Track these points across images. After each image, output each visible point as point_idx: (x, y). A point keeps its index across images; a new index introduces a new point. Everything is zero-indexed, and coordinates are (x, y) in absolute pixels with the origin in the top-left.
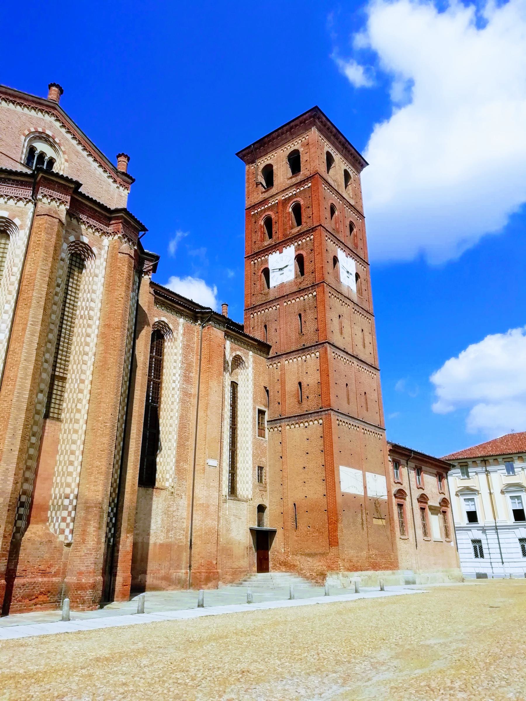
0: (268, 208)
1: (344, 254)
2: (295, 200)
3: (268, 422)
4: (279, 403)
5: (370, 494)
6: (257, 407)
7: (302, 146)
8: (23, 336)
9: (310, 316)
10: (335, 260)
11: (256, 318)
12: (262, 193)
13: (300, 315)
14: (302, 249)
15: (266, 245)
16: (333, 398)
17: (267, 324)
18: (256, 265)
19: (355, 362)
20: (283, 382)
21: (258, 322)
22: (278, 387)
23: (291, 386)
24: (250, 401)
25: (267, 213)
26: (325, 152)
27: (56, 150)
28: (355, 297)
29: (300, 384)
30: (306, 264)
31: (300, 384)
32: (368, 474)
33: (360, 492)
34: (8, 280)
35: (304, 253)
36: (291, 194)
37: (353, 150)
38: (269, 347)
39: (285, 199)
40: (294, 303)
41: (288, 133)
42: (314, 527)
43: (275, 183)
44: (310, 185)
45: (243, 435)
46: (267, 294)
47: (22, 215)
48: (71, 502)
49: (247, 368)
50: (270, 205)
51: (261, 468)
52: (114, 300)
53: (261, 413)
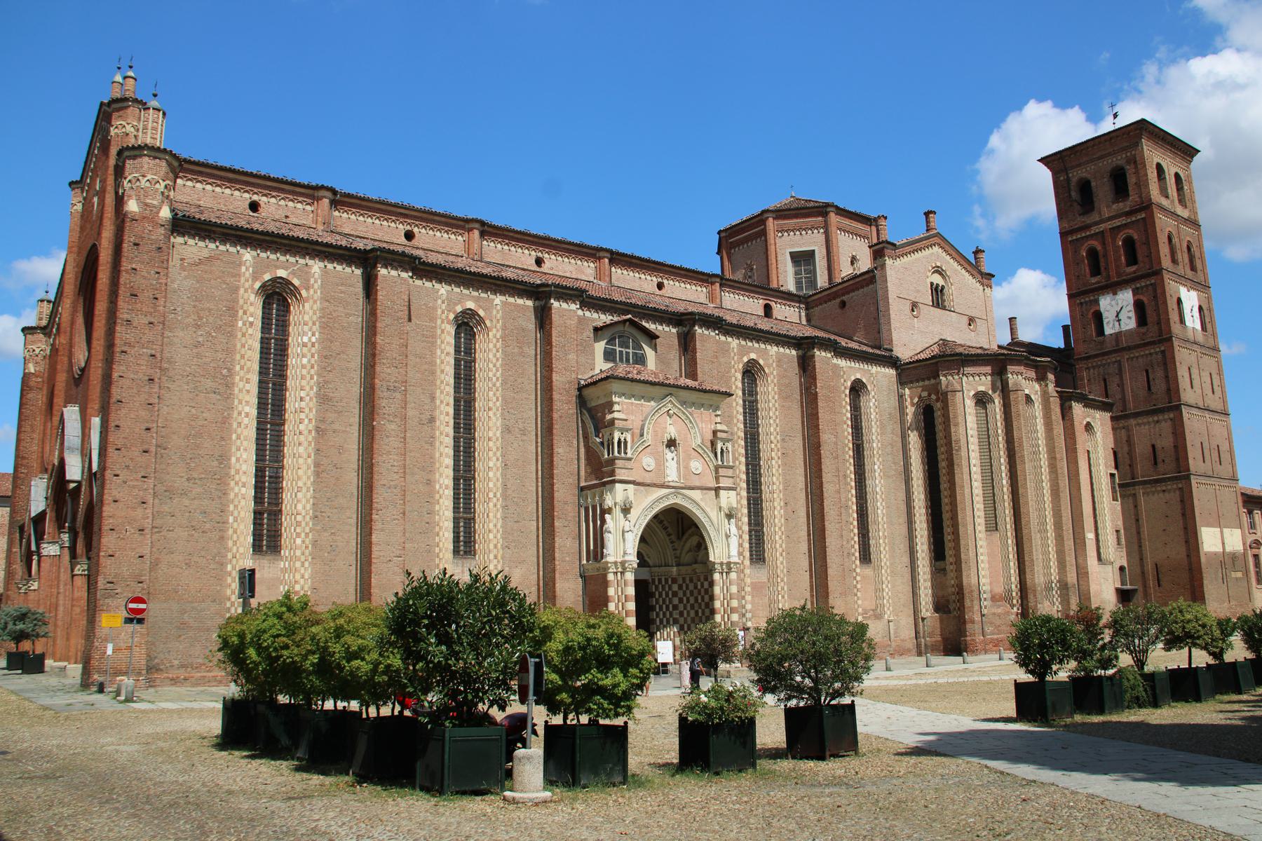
0: (1091, 236)
1: (1186, 289)
5: (1228, 549)
6: (1109, 472)
7: (1128, 162)
8: (1026, 484)
9: (1158, 374)
10: (1179, 301)
12: (1080, 215)
13: (1147, 371)
14: (1142, 294)
16: (1191, 461)
19: (1207, 416)
20: (1129, 442)
22: (1126, 449)
23: (1141, 448)
24: (1102, 467)
26: (1155, 166)
27: (943, 277)
28: (1200, 337)
29: (1153, 446)
30: (1149, 312)
31: (1153, 446)
32: (1225, 530)
33: (1219, 549)
35: (1145, 299)
36: (1119, 224)
37: (1182, 145)
39: (1113, 229)
41: (1107, 143)
42: (1179, 585)
43: (1096, 204)
44: (1143, 216)
46: (1102, 343)
48: (1056, 585)
50: (1092, 232)
51: (1117, 531)
53: (1112, 475)
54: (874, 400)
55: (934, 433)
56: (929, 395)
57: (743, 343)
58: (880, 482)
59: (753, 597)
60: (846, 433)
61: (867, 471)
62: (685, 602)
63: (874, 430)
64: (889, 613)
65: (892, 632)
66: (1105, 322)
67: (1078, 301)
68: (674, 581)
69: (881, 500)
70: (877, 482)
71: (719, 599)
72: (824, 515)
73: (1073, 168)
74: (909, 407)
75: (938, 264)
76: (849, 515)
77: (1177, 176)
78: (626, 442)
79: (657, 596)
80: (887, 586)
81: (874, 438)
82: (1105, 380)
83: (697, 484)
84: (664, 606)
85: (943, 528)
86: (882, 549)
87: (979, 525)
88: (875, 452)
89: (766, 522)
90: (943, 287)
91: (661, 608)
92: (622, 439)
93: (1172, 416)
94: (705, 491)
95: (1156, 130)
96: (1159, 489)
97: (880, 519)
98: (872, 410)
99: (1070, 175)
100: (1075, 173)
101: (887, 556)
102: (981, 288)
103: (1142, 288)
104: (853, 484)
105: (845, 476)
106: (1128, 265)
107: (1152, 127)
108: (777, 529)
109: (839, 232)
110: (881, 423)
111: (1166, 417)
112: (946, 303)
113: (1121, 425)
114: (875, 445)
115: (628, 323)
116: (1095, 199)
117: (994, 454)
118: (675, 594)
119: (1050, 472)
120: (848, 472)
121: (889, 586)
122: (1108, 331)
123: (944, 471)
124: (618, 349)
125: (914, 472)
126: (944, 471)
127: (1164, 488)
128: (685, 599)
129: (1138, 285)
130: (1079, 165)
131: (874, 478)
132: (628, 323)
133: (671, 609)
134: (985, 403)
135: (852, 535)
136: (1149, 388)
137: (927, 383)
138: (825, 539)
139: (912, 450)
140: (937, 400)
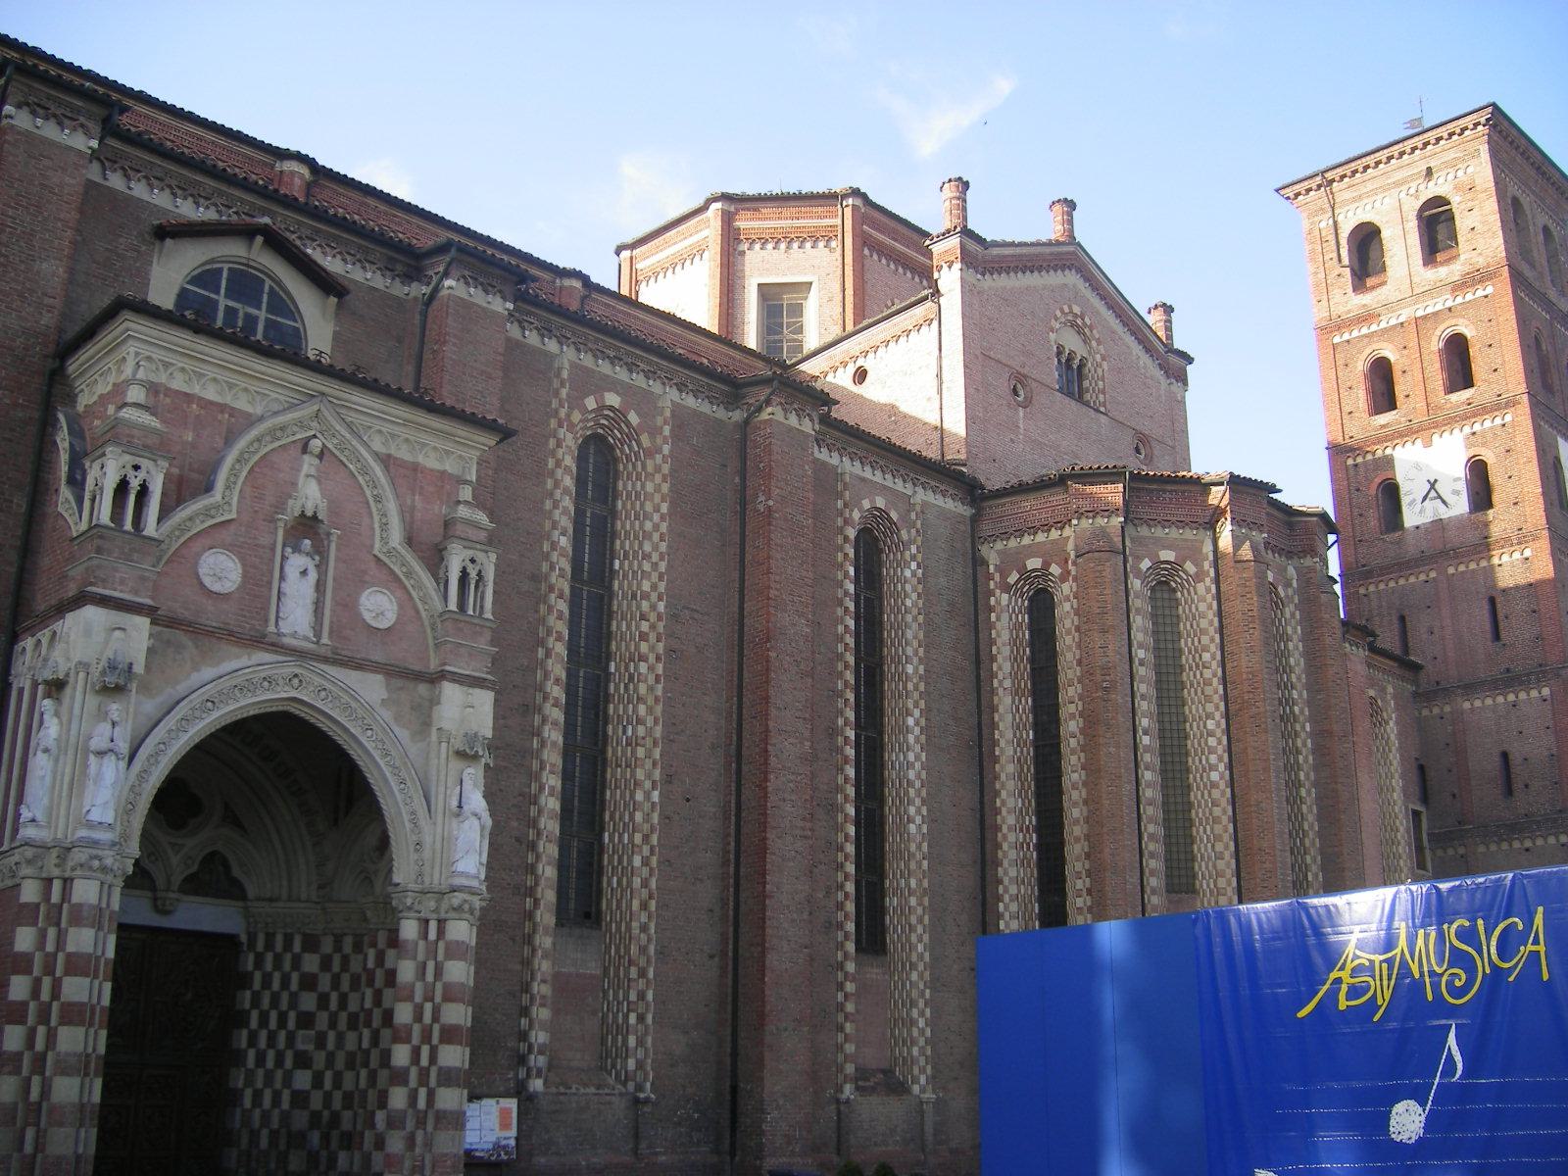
2: (1453, 322)
3: (1428, 834)
4: (1454, 796)
6: (1411, 806)
11: (1372, 596)
14: (1484, 444)
15: (1382, 423)
17: (1406, 613)
18: (1362, 470)
21: (1380, 607)
23: (1483, 762)
25: (1375, 347)
29: (1505, 755)
30: (1496, 478)
31: (1505, 755)
34: (1198, 676)
35: (1489, 456)
36: (1439, 307)
38: (1415, 668)
39: (1425, 317)
40: (1473, 571)
44: (1490, 290)
45: (1393, 869)
46: (1399, 542)
47: (1196, 557)
49: (1387, 723)
50: (1383, 325)
52: (1330, 684)
53: (1416, 814)
54: (914, 565)
55: (1053, 655)
56: (1046, 565)
57: (587, 360)
58: (917, 758)
59: (556, 1012)
60: (840, 629)
61: (888, 729)
62: (334, 1005)
63: (909, 634)
64: (923, 1080)
65: (929, 1128)
66: (1405, 501)
67: (1350, 462)
68: (311, 944)
69: (918, 802)
70: (911, 757)
71: (410, 998)
72: (765, 814)
73: (1346, 202)
74: (998, 591)
75: (1077, 310)
76: (838, 828)
77: (1546, 230)
78: (143, 491)
79: (257, 986)
80: (922, 1014)
81: (909, 651)
82: (1402, 619)
83: (378, 656)
84: (274, 1015)
85: (1064, 881)
86: (913, 920)
87: (1152, 873)
88: (910, 686)
89: (612, 818)
90: (1081, 366)
91: (264, 1021)
92: (135, 484)
93: (1546, 691)
94: (399, 683)
95: (1514, 132)
96: (1516, 844)
97: (913, 847)
98: (908, 587)
99: (1340, 219)
100: (1350, 214)
101: (926, 938)
102: (1164, 381)
103: (1484, 432)
104: (850, 752)
105: (833, 732)
106: (1451, 388)
107: (1506, 123)
108: (638, 838)
109: (866, 252)
110: (928, 622)
111: (1534, 693)
112: (1087, 397)
113: (1436, 711)
114: (910, 669)
115: (259, 239)
116: (1388, 263)
117: (1192, 709)
118: (309, 983)
119: (1316, 768)
120: (840, 721)
121: (928, 1012)
122: (1412, 517)
123: (1073, 742)
124: (223, 302)
125: (1002, 743)
126: (1073, 742)
127: (1528, 844)
128: (334, 997)
129: (1477, 427)
130: (1360, 197)
131: (905, 748)
132: (259, 239)
133: (291, 1024)
134: (1174, 591)
135: (840, 877)
136: (1497, 636)
137: (1041, 537)
138: (764, 875)
139: (1001, 691)
140: (1064, 578)
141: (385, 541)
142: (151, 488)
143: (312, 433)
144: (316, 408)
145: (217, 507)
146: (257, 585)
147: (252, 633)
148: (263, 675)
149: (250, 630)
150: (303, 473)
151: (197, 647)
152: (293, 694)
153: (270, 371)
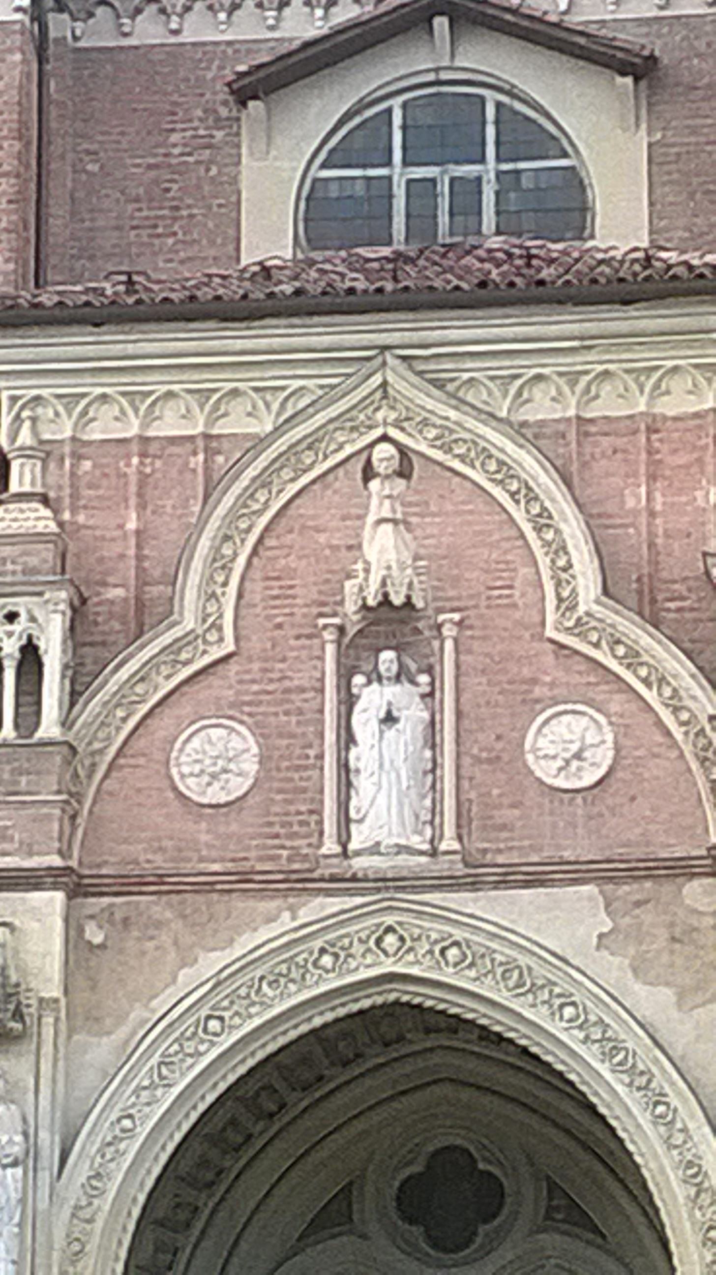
141: (567, 604)
142: (42, 645)
143: (378, 432)
144: (377, 379)
145: (188, 639)
146: (298, 768)
147: (296, 866)
148: (318, 944)
149: (290, 859)
150: (371, 519)
151: (184, 917)
152: (388, 966)
153: (263, 343)
